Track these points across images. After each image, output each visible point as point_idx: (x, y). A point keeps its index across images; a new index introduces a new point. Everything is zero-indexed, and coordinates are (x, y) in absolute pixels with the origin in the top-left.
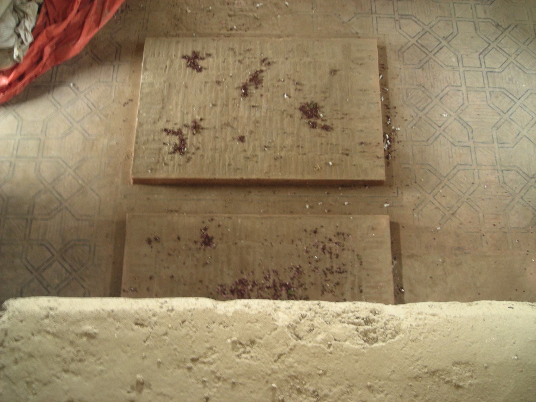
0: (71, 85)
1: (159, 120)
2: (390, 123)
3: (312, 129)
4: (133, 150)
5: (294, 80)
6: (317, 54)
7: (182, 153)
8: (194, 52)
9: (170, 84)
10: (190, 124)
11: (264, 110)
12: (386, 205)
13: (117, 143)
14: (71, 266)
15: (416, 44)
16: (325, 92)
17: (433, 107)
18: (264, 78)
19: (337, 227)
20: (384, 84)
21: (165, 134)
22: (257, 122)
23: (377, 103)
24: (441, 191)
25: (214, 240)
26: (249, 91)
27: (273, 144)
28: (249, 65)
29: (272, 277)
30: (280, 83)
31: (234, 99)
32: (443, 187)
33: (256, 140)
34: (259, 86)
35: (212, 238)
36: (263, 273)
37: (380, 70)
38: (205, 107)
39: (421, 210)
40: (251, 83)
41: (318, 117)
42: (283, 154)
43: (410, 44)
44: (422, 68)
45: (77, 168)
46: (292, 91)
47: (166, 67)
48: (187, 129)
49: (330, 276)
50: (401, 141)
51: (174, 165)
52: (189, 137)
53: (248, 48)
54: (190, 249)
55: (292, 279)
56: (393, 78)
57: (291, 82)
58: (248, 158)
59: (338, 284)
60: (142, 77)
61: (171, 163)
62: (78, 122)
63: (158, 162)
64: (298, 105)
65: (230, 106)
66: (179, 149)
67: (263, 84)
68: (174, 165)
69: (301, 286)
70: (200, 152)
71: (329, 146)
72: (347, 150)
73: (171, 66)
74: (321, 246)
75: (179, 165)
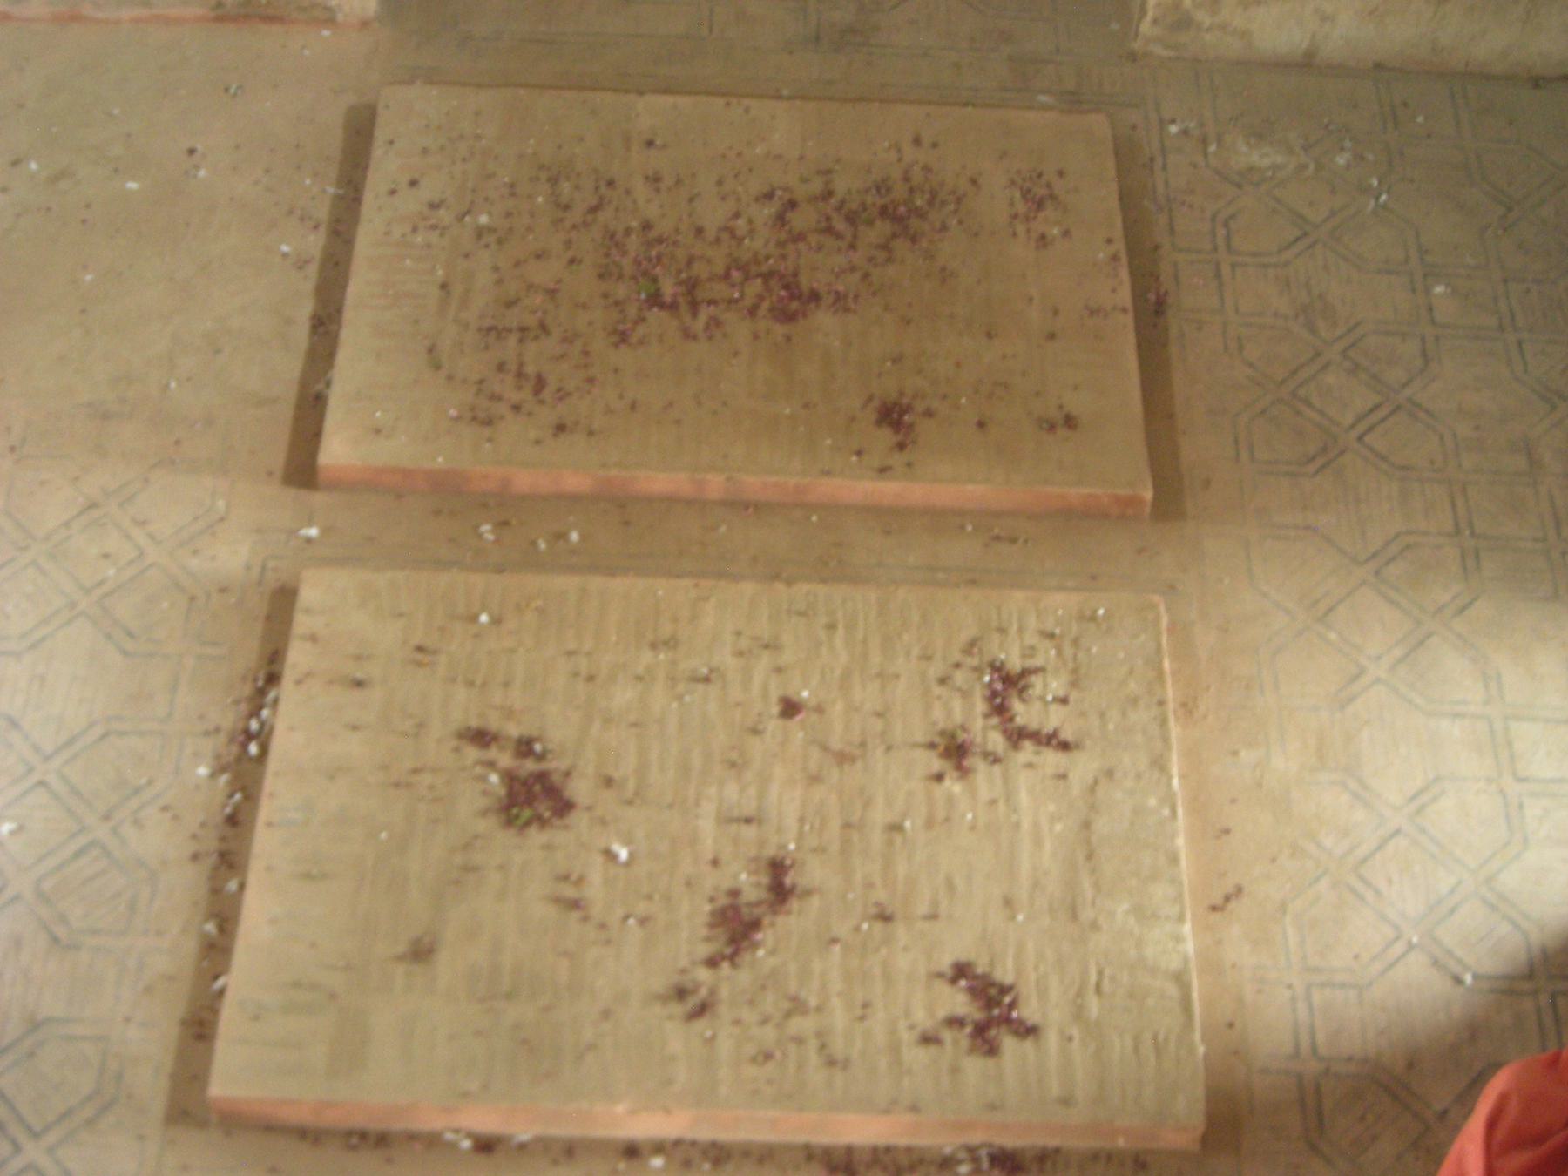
0: (1468, 978)
1: (1096, 782)
2: (231, 796)
3: (535, 733)
4: (1175, 730)
5: (586, 919)
6: (478, 1033)
7: (997, 668)
8: (992, 1050)
9: (1074, 915)
10: (974, 761)
11: (708, 809)
12: (313, 532)
13: (1235, 753)
14: (1298, 413)
15: (22, 1138)
16: (468, 869)
17: (41, 859)
18: (704, 932)
19: (490, 440)
20: (216, 951)
21: (1067, 734)
22: (733, 765)
23: (269, 824)
24: (111, 572)
25: (873, 417)
26: (765, 879)
27: (681, 687)
28: (763, 988)
29: (699, 324)
30: (642, 908)
31: (820, 850)
32: (101, 583)
33: (738, 704)
34: (723, 901)
35: (879, 423)
36: (725, 335)
37: (214, 1011)
38: (929, 824)
39: (196, 518)
40: (757, 911)
41: (509, 777)
42: (647, 657)
43: (51, 1138)
44: (35, 1024)
45: (1356, 678)
46: (596, 876)
47: (1098, 989)
48: (990, 747)
49: (531, 321)
50: (207, 733)
51: (1021, 630)
52: (978, 723)
53: (770, 1067)
54: (944, 397)
55: (642, 320)
56: (171, 978)
57: (596, 911)
58: (766, 647)
59: (510, 304)
60: (1190, 947)
61: (1031, 638)
62: (1398, 832)
63: (1076, 642)
64: (578, 819)
65: (835, 825)
66: (1008, 684)
67: (708, 908)
68: (1021, 630)
69: (617, 303)
70: (935, 670)
71: (478, 682)
72: (420, 664)
73: (1080, 994)
74: (547, 394)
75: (1002, 630)
